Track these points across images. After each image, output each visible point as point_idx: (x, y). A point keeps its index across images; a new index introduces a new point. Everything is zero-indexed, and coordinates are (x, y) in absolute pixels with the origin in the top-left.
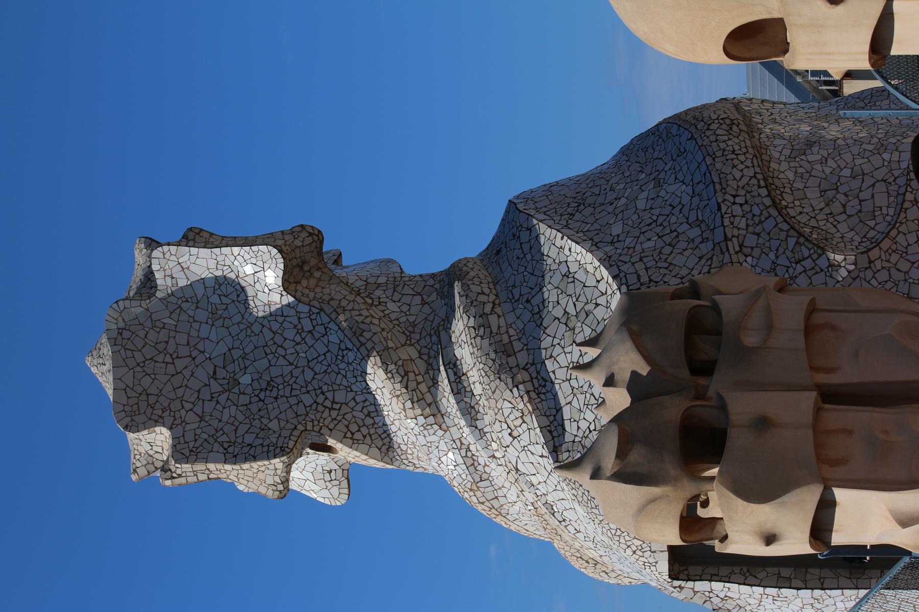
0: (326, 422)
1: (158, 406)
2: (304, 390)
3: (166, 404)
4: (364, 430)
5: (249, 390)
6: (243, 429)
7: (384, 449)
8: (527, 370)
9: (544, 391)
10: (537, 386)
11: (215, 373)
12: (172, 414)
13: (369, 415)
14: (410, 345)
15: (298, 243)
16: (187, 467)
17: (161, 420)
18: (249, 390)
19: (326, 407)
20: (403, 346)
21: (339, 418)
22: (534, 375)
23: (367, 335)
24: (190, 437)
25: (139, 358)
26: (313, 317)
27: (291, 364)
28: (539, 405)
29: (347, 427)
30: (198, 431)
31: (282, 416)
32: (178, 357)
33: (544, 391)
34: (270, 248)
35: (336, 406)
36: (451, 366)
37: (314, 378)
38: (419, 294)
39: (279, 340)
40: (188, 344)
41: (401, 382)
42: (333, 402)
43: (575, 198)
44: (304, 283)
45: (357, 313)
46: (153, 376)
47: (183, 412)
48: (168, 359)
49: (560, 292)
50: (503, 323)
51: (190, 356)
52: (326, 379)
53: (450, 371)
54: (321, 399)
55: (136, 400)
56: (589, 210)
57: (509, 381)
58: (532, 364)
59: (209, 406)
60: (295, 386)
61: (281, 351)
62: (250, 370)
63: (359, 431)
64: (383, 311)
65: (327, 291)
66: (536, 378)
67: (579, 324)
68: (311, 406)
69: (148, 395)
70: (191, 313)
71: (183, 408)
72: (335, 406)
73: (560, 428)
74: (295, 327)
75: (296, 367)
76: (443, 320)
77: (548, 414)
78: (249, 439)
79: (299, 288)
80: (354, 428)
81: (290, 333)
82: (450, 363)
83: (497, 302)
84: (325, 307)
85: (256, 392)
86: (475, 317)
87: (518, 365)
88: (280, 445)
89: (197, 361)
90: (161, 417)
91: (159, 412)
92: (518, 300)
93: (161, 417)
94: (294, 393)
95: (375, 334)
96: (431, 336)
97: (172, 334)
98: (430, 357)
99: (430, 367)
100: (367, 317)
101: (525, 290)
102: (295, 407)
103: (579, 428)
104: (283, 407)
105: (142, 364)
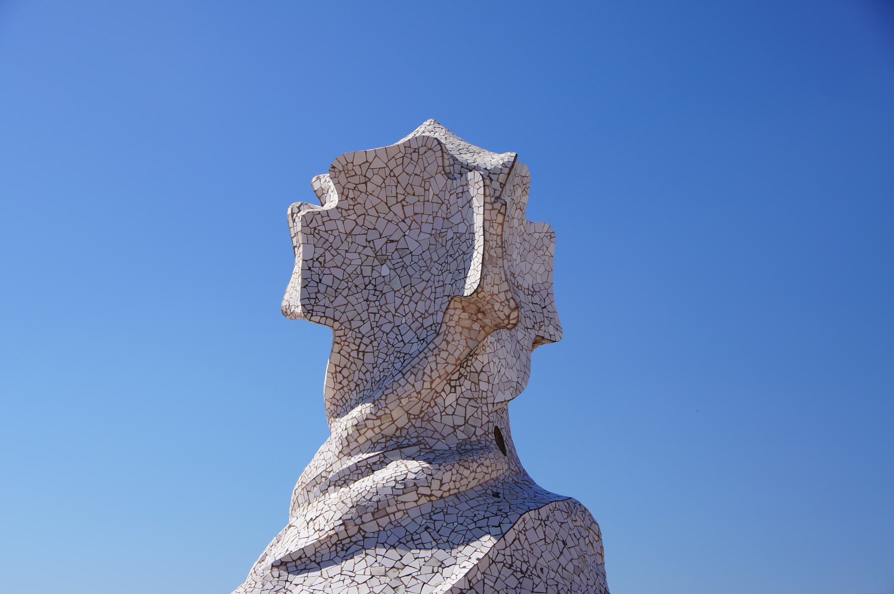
0: (345, 348)
1: (357, 193)
2: (374, 324)
3: (359, 200)
4: (345, 382)
5: (375, 274)
6: (338, 273)
7: (335, 401)
8: (359, 532)
9: (339, 549)
10: (343, 542)
11: (392, 241)
12: (351, 207)
13: (357, 385)
14: (409, 419)
15: (497, 306)
16: (299, 227)
17: (344, 197)
18: (375, 274)
19: (359, 346)
20: (407, 412)
21: (351, 359)
22: (354, 539)
23: (412, 379)
24: (330, 226)
25: (398, 171)
26: (434, 327)
27: (396, 311)
28: (325, 546)
29: (345, 367)
30: (336, 233)
31: (350, 307)
32: (403, 206)
33: (339, 549)
34: (478, 282)
35: (361, 356)
36: (382, 459)
37: (384, 332)
38: (466, 422)
39: (417, 297)
40: (416, 214)
41: (371, 413)
42: (364, 352)
43: (535, 567)
44: (465, 316)
45: (434, 367)
46: (383, 185)
47: (354, 217)
48: (400, 198)
49: (427, 559)
50: (408, 506)
51: (406, 218)
52: (383, 344)
53: (377, 458)
54: (366, 341)
55: (359, 173)
56: (513, 582)
57: (349, 516)
58: (364, 537)
59: (361, 240)
60: (378, 316)
61: (407, 300)
62: (393, 274)
63: (344, 378)
64: (443, 390)
65: (457, 337)
66: (351, 541)
67: (387, 580)
68: (360, 332)
69: (366, 183)
70: (439, 214)
71: (358, 217)
72: (361, 354)
73: (303, 566)
74: (426, 311)
75: (394, 316)
76: (431, 448)
77: (318, 554)
78: (327, 280)
79: (459, 312)
80: (345, 372)
81: (421, 307)
82: (385, 457)
83: (433, 498)
84: (441, 337)
85: (373, 282)
86: (415, 479)
87: (363, 523)
88: (315, 308)
89: (401, 224)
90: (347, 197)
91: (351, 195)
92: (431, 519)
93: (347, 197)
94: (372, 316)
95: (413, 386)
96: (417, 437)
97: (422, 199)
98: (397, 438)
99: (388, 438)
100: (431, 377)
101: (438, 525)
102: (358, 318)
103: (296, 585)
104: (358, 307)
105: (392, 174)
